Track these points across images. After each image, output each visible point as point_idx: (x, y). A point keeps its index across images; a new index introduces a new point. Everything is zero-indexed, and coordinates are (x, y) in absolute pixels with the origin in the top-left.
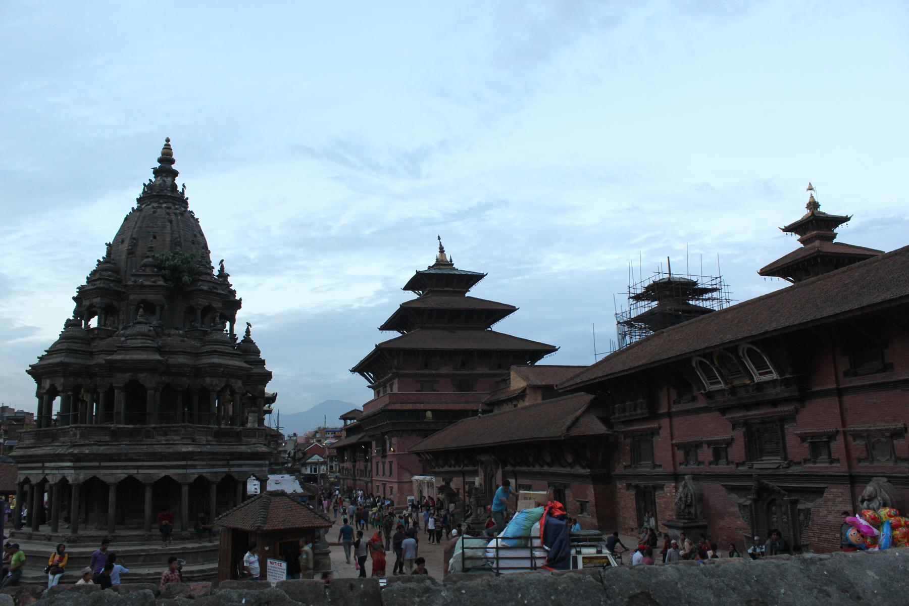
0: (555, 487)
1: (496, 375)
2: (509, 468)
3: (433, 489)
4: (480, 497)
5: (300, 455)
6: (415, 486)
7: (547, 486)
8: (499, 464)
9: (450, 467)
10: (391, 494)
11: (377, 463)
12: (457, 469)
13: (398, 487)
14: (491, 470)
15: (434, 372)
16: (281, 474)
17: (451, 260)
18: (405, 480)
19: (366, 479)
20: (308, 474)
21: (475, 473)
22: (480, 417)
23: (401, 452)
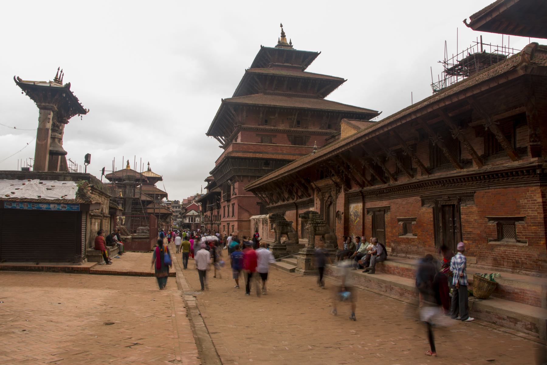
0: (436, 203)
1: (326, 134)
2: (355, 189)
3: (267, 226)
4: (318, 223)
5: (184, 211)
6: (252, 223)
7: (420, 203)
8: (341, 188)
9: (284, 201)
10: (233, 231)
11: (224, 207)
12: (291, 201)
13: (238, 225)
14: (330, 196)
15: (273, 128)
16: (64, 180)
17: (291, 43)
18: (244, 220)
19: (218, 222)
20: (187, 223)
21: (311, 203)
22: (314, 153)
23: (241, 194)
